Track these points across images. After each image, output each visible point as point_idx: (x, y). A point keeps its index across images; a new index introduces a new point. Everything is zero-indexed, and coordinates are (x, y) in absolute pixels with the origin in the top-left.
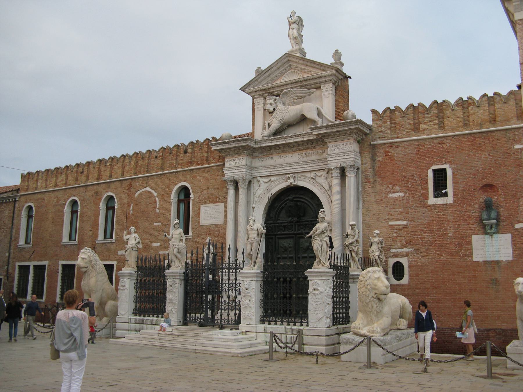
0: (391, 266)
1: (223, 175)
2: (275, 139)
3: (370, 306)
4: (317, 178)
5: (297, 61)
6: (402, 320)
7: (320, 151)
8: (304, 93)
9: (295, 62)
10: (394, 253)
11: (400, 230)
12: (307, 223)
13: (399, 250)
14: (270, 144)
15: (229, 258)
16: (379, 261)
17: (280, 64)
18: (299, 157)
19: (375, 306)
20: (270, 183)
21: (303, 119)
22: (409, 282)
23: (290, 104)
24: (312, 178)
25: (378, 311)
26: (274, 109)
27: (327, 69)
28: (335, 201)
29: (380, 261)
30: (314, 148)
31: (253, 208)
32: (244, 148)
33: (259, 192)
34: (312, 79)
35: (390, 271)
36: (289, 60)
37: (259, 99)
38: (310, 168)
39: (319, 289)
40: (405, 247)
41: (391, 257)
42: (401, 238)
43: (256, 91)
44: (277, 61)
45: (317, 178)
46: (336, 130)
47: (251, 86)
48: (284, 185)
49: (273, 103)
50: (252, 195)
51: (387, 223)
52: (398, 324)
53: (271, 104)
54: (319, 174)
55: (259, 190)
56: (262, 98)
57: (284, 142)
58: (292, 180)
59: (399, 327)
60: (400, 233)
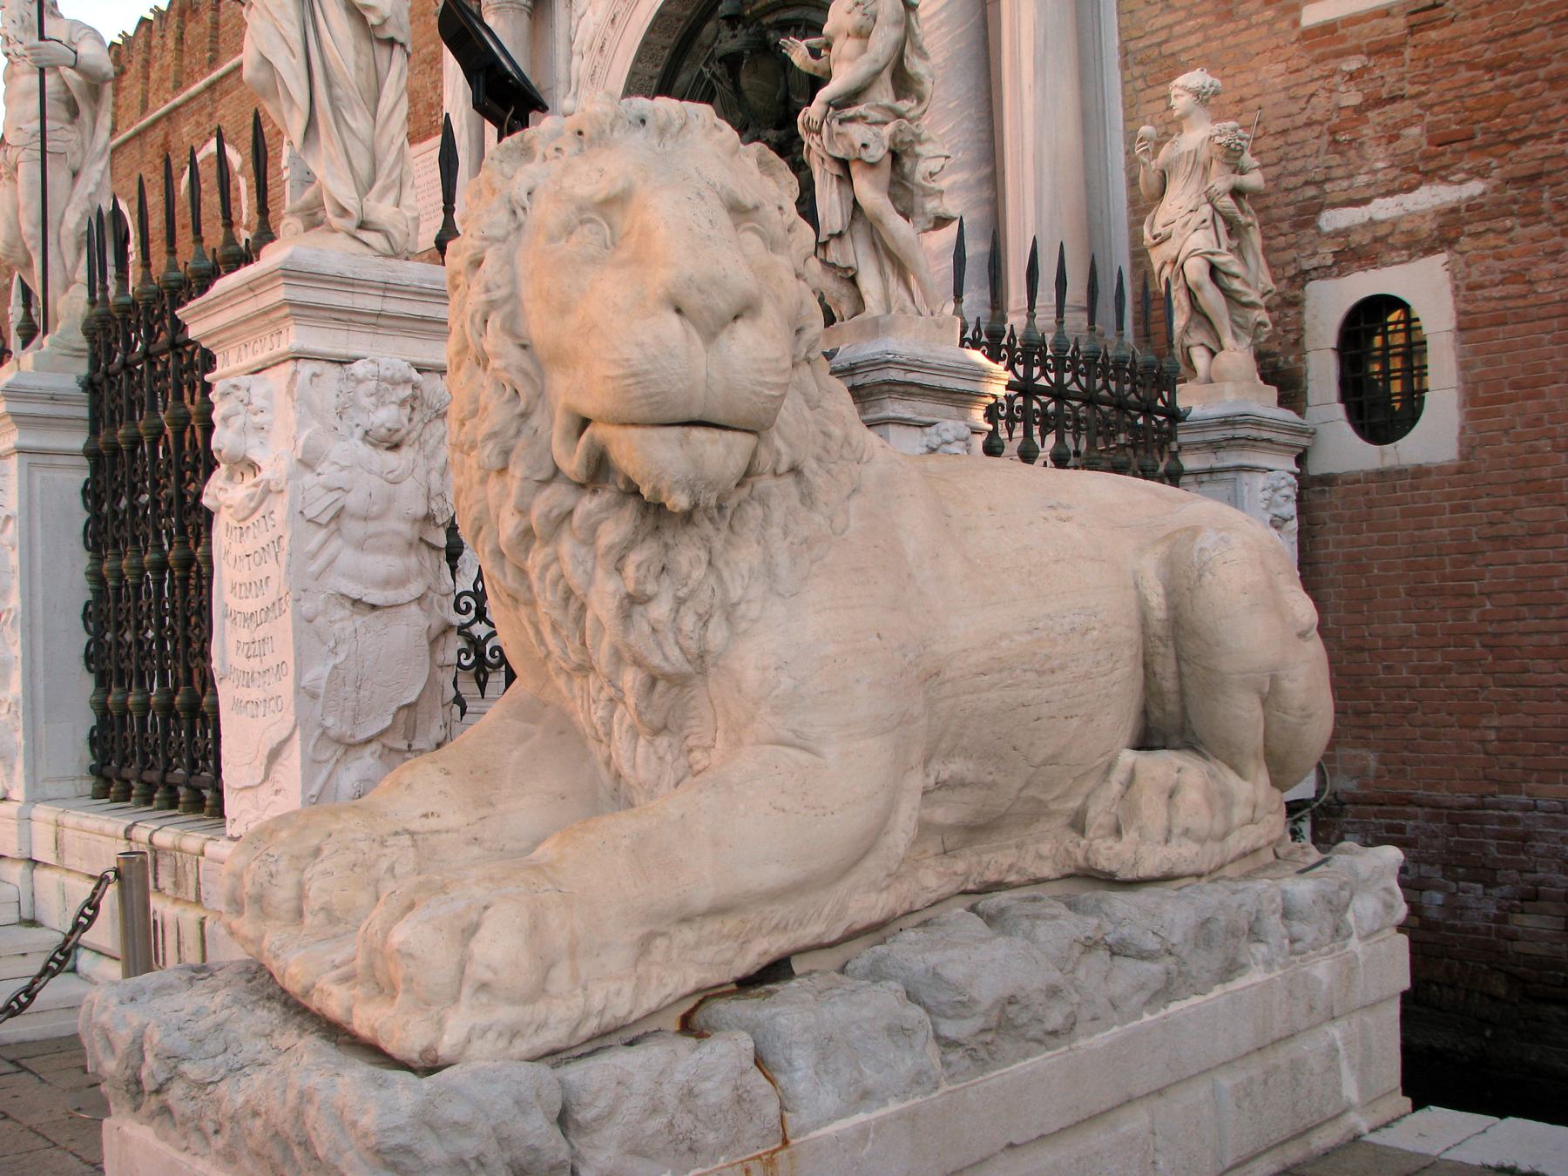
0: (1332, 339)
3: (547, 600)
6: (1161, 765)
10: (1345, 233)
11: (1385, 50)
13: (1383, 209)
16: (1211, 297)
19: (604, 597)
22: (1468, 448)
25: (672, 658)
29: (1228, 294)
35: (1322, 371)
39: (255, 455)
40: (1428, 176)
41: (1324, 272)
42: (1396, 111)
50: (561, 48)
51: (1284, 25)
52: (1099, 815)
59: (1108, 854)
60: (1389, 75)
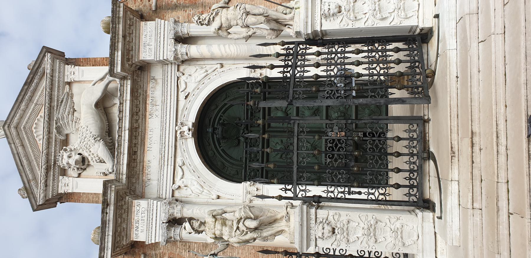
1: (156, 244)
2: (120, 145)
4: (188, 90)
5: (20, 112)
7: (151, 85)
8: (67, 101)
9: (21, 117)
12: (249, 111)
14: (126, 156)
15: (272, 67)
17: (17, 141)
18: (154, 116)
20: (184, 168)
21: (102, 106)
23: (77, 127)
24: (186, 97)
26: (80, 154)
27: (43, 66)
28: (220, 50)
30: (146, 92)
31: (218, 197)
32: (119, 198)
33: (195, 187)
34: (52, 89)
36: (16, 128)
37: (60, 184)
38: (172, 100)
43: (46, 186)
44: (9, 143)
45: (188, 90)
46: (121, 39)
47: (35, 190)
48: (191, 144)
49: (69, 153)
53: (69, 157)
54: (182, 87)
55: (193, 188)
56: (61, 177)
57: (127, 132)
58: (185, 129)
